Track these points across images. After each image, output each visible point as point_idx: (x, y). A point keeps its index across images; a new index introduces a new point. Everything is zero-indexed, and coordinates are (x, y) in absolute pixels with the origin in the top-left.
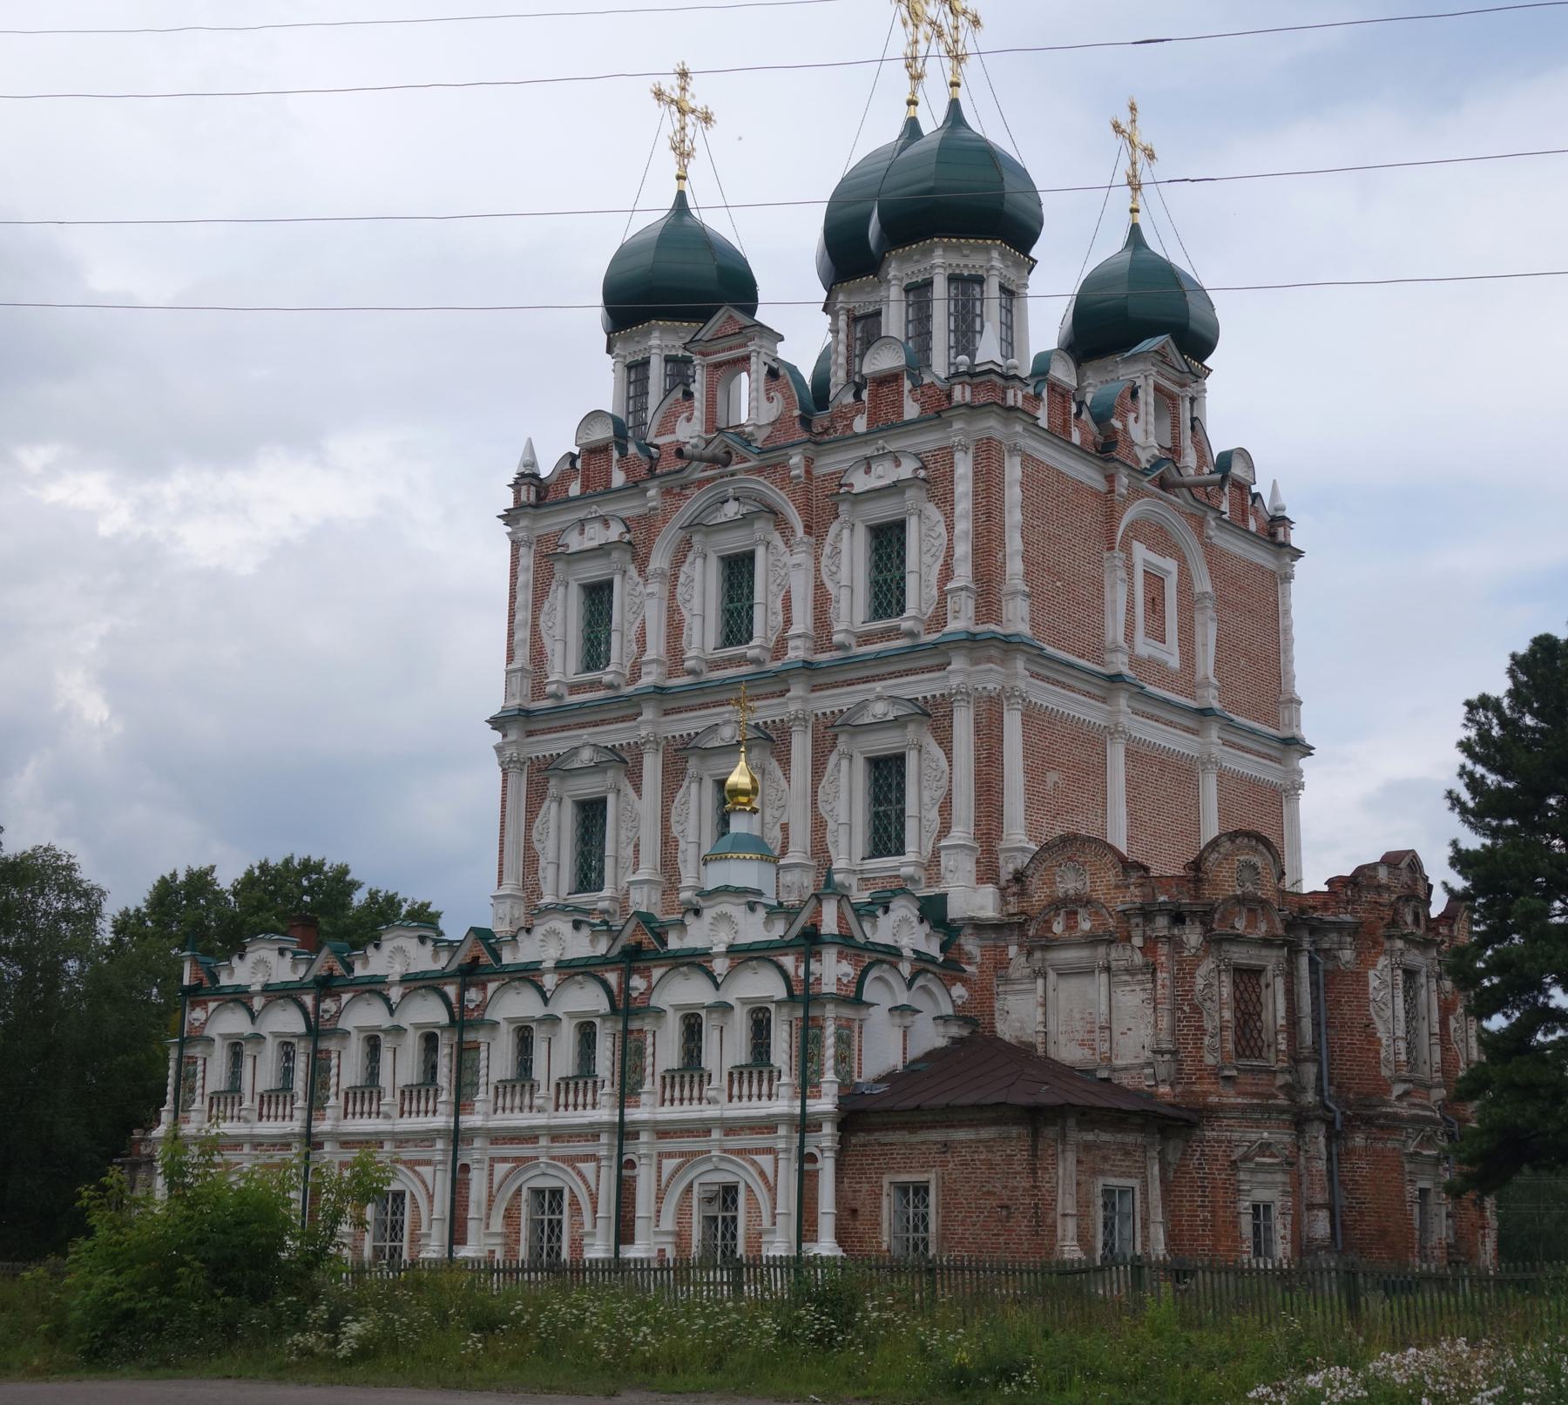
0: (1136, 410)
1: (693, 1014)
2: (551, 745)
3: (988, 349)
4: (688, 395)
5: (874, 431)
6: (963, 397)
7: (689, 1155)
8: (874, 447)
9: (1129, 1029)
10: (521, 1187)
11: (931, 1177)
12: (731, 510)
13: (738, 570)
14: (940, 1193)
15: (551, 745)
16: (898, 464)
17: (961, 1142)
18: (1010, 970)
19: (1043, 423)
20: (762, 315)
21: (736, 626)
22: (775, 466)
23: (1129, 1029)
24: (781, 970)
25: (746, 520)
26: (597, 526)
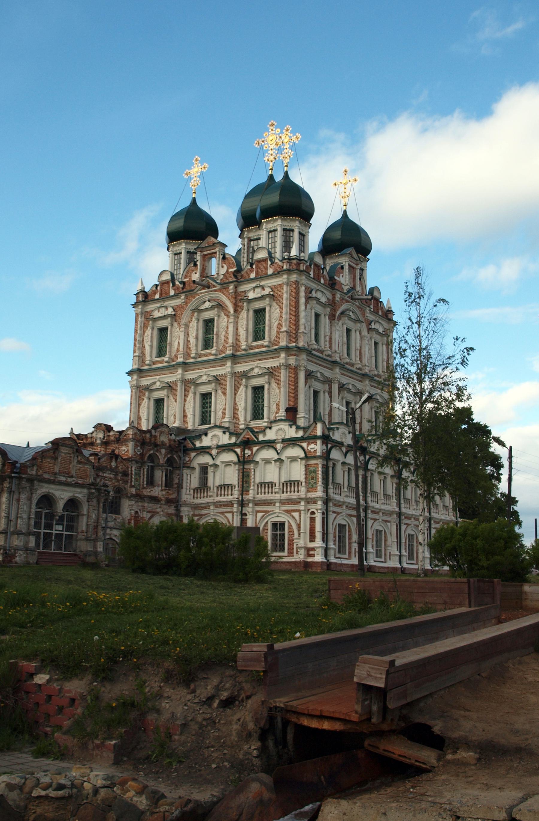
0: (342, 273)
2: (145, 382)
3: (294, 252)
4: (195, 265)
7: (266, 512)
10: (267, 521)
13: (209, 324)
15: (145, 382)
19: (312, 276)
20: (221, 238)
21: (258, 335)
24: (302, 447)
26: (163, 309)
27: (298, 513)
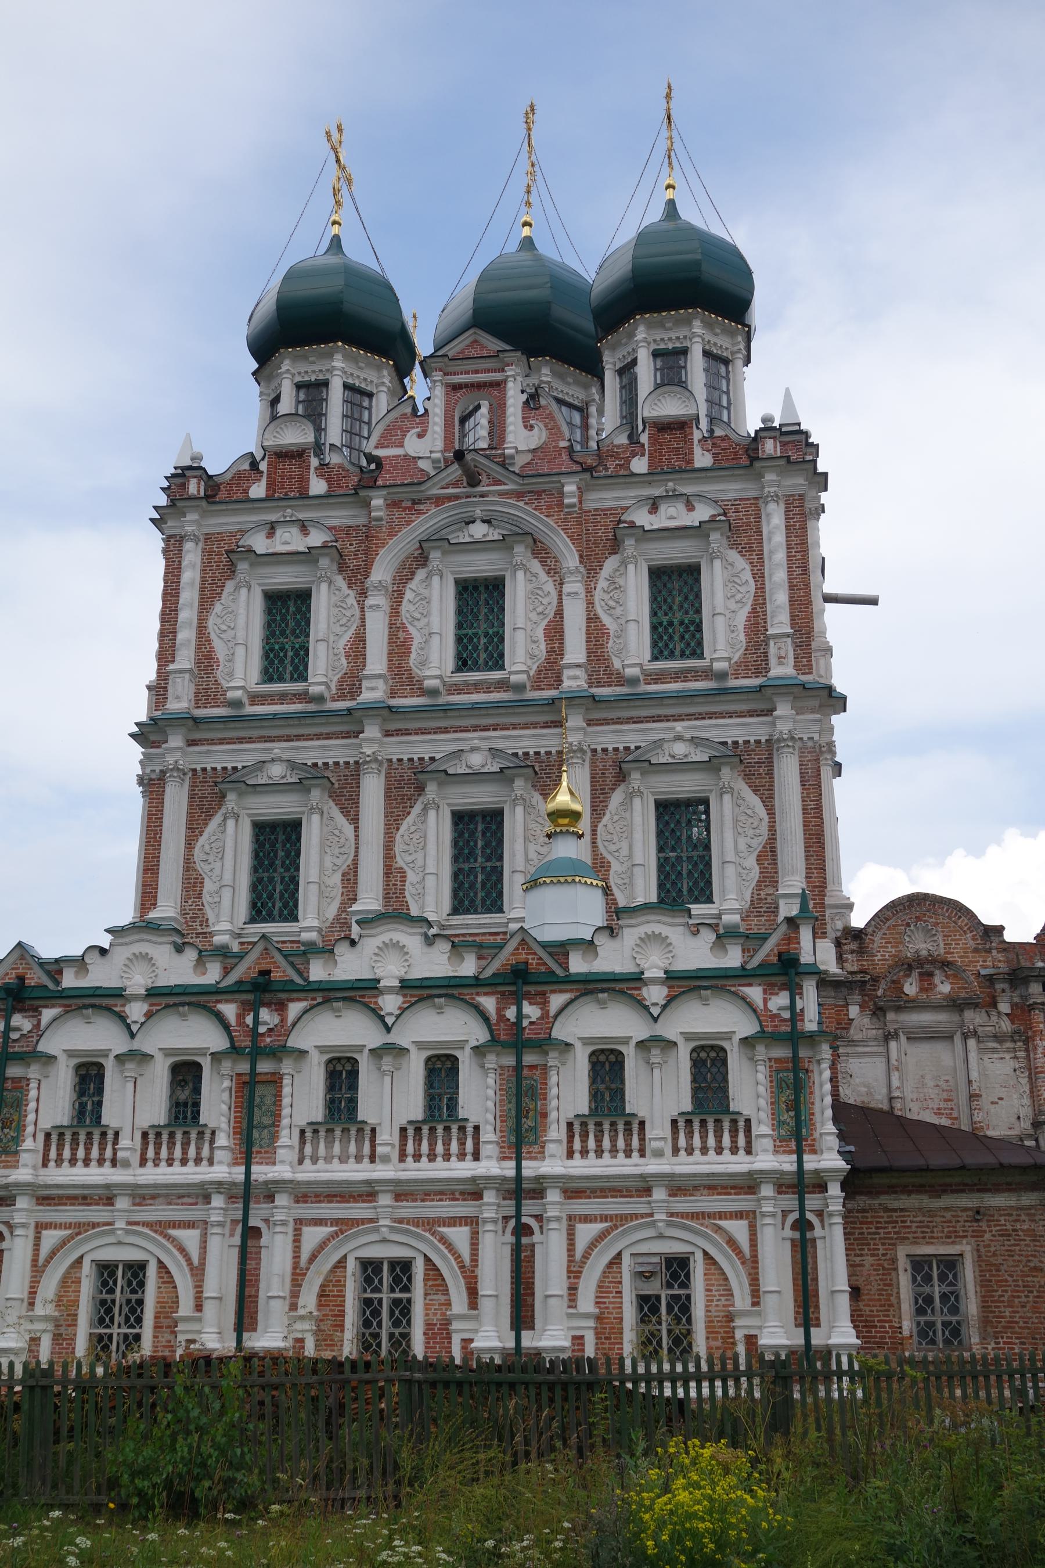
1: (612, 1051)
5: (655, 472)
6: (775, 451)
8: (663, 488)
9: (1001, 1099)
11: (966, 1248)
12: (479, 531)
14: (977, 1269)
16: (690, 507)
17: (999, 1209)
18: (852, 1031)
22: (539, 493)
23: (1001, 1099)
25: (504, 544)
27: (466, 1229)
